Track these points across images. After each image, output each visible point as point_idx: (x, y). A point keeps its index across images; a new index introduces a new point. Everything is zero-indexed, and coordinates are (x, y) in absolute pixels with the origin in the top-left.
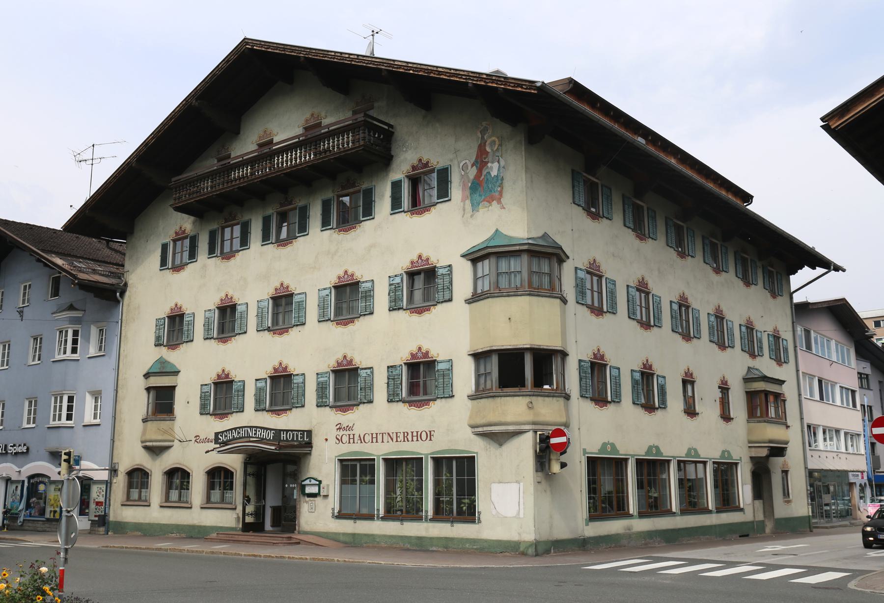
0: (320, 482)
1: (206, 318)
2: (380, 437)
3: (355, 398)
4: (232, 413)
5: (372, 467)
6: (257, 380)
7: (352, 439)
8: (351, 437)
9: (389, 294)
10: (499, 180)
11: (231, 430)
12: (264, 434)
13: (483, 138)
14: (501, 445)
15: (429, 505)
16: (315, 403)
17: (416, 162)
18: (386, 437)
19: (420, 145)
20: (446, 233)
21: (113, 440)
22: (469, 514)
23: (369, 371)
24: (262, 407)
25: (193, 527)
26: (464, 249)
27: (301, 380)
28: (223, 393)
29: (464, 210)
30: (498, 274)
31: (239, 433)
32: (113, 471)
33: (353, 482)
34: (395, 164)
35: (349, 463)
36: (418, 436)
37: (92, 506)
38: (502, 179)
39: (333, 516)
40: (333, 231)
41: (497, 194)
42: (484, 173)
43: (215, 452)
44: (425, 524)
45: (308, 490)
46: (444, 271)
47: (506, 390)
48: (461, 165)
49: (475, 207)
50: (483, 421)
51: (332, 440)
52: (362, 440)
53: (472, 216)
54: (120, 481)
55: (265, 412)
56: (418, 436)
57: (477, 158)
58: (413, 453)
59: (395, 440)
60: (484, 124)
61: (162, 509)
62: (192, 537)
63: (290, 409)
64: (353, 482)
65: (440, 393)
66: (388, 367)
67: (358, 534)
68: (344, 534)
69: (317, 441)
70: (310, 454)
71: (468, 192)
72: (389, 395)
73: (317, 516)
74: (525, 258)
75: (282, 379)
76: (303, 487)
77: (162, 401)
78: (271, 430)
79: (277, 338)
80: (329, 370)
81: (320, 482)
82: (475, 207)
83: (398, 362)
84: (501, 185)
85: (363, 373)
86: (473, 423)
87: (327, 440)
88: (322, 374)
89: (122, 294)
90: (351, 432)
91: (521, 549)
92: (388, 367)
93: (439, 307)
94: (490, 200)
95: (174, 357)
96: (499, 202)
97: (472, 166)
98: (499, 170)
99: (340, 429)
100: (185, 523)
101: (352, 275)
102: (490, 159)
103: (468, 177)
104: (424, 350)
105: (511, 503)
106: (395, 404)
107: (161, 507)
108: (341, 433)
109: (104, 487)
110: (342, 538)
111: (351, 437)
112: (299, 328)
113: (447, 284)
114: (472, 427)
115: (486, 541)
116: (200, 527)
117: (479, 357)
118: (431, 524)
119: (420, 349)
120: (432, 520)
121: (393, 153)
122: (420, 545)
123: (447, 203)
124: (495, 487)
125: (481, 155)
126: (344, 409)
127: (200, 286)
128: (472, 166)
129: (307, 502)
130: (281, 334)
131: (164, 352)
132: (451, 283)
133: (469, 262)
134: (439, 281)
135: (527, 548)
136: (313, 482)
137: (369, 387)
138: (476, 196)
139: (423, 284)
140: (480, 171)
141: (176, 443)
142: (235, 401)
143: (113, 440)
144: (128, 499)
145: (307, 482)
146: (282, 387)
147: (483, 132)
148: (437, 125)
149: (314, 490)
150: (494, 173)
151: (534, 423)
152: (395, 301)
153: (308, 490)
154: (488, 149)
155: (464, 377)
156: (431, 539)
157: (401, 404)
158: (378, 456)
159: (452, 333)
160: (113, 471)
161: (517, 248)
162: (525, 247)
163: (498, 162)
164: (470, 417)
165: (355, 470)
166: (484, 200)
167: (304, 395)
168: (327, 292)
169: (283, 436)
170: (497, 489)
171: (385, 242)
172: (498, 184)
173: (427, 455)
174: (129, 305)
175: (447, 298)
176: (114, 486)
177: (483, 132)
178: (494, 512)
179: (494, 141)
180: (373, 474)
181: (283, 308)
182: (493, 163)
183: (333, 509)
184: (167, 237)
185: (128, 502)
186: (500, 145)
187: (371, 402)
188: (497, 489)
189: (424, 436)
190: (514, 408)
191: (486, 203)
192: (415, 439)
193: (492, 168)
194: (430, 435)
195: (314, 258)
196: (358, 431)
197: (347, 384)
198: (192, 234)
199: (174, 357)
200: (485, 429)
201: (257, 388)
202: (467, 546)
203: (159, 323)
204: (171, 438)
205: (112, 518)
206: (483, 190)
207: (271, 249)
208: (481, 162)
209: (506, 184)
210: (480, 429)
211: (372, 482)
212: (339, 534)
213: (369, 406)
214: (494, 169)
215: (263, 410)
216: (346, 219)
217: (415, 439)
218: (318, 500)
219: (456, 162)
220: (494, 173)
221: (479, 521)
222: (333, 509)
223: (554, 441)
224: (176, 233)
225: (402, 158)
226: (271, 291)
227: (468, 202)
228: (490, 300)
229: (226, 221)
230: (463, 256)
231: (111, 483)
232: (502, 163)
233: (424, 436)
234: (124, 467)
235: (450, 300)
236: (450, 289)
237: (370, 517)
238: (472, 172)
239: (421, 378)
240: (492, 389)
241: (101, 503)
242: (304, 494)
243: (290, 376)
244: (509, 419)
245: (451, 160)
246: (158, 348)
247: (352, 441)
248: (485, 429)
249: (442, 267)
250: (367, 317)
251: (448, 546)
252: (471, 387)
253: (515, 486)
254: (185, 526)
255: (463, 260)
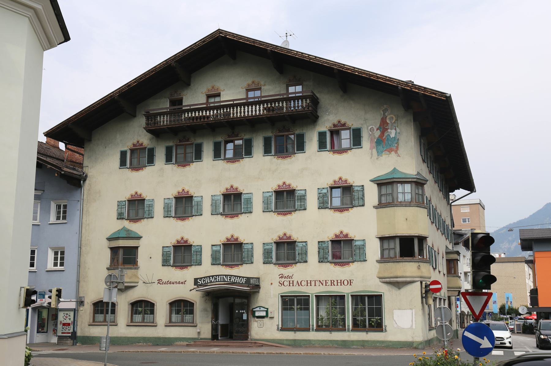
0: (267, 309)
1: (165, 203)
2: (313, 283)
3: (295, 259)
4: (191, 265)
5: (308, 300)
6: (213, 245)
7: (291, 284)
8: (291, 282)
9: (318, 199)
10: (396, 140)
11: (209, 277)
12: (238, 280)
13: (384, 114)
14: (399, 288)
15: (349, 322)
16: (261, 261)
17: (336, 122)
18: (317, 283)
19: (335, 112)
20: (361, 166)
21: (78, 281)
22: (378, 326)
23: (304, 244)
24: (218, 262)
25: (159, 339)
26: (373, 177)
27: (251, 247)
28: (182, 254)
29: (372, 154)
30: (392, 194)
31: (215, 279)
32: (81, 303)
33: (292, 309)
34: (320, 121)
35: (303, 298)
36: (342, 283)
37: (60, 327)
38: (398, 140)
39: (278, 329)
40: (272, 157)
41: (395, 148)
42: (386, 134)
43: (195, 290)
44: (348, 333)
45: (257, 314)
46: (359, 189)
47: (405, 258)
48: (369, 128)
49: (379, 153)
51: (276, 284)
52: (300, 284)
53: (377, 159)
54: (87, 311)
55: (220, 266)
56: (342, 283)
57: (380, 125)
58: (334, 292)
59: (324, 284)
60: (385, 106)
61: (129, 327)
62: (158, 345)
63: (242, 264)
64: (292, 309)
65: (358, 258)
66: (319, 242)
67: (298, 340)
68: (287, 340)
69: (264, 285)
70: (258, 292)
71: (374, 145)
72: (320, 258)
74: (414, 185)
75: (286, 245)
76: (253, 313)
77: (124, 255)
78: (243, 277)
79: (229, 220)
80: (273, 242)
81: (267, 309)
82: (379, 153)
83: (326, 239)
84: (397, 143)
86: (381, 276)
87: (272, 284)
88: (267, 244)
89: (85, 180)
90: (291, 280)
91: (414, 346)
92: (319, 242)
93: (355, 209)
94: (390, 151)
95: (135, 227)
96: (396, 152)
97: (377, 129)
98: (396, 134)
99: (282, 277)
100: (151, 336)
101: (289, 185)
102: (390, 127)
103: (374, 136)
104: (185, 239)
105: (405, 320)
106: (324, 263)
107: (128, 326)
108: (283, 280)
109: (72, 314)
110: (285, 342)
111: (291, 282)
112: (247, 215)
113: (361, 196)
114: (380, 278)
115: (390, 342)
116: (166, 338)
117: (382, 239)
118: (352, 333)
119: (182, 238)
120: (352, 330)
121: (318, 114)
123: (360, 149)
124: (397, 313)
125: (383, 124)
126: (285, 265)
127: (160, 181)
128: (377, 129)
129: (256, 321)
130: (232, 217)
131: (126, 224)
132: (363, 195)
133: (376, 185)
134: (355, 194)
135: (419, 345)
136: (262, 309)
137: (305, 253)
138: (380, 147)
139: (347, 194)
140: (383, 133)
141: (140, 284)
142: (194, 258)
143: (78, 281)
144: (94, 321)
145: (258, 309)
146: (234, 251)
147: (385, 111)
148: (351, 102)
149: (264, 314)
150: (393, 135)
151: (421, 277)
152: (323, 203)
153: (257, 314)
154: (388, 121)
155: (373, 250)
156: (352, 341)
157: (328, 264)
158: (312, 294)
159: (365, 224)
160: (81, 303)
161: (410, 180)
162: (415, 180)
163: (395, 129)
164: (379, 272)
165: (288, 302)
166: (386, 150)
167: (252, 256)
168: (270, 194)
169: (252, 281)
170: (397, 313)
171: (312, 168)
172: (395, 142)
173: (348, 294)
174: (89, 190)
175: (361, 204)
176: (80, 313)
177: (385, 111)
178: (395, 326)
179: (392, 118)
180: (308, 304)
181: (233, 202)
182: (391, 129)
183: (278, 326)
184: (127, 146)
185: (94, 323)
186: (397, 120)
187: (306, 262)
188: (397, 313)
189: (346, 283)
190: (408, 269)
191: (387, 152)
193: (391, 133)
194: (350, 282)
195: (259, 172)
196: (295, 279)
197: (286, 251)
198: (150, 146)
199: (135, 227)
200: (392, 279)
201: (213, 251)
202: (378, 345)
203: (120, 204)
204: (136, 281)
205: (79, 334)
206: (384, 144)
207: (220, 164)
208: (383, 127)
209: (401, 143)
210: (383, 280)
211: (308, 309)
212: (284, 340)
213: (305, 264)
214: (392, 133)
215: (219, 264)
216: (283, 151)
218: (265, 320)
219: (365, 126)
220: (393, 135)
221: (386, 331)
222: (278, 326)
223: (432, 287)
224: (134, 145)
225: (326, 118)
226: (223, 190)
227: (374, 151)
228: (395, 208)
229: (180, 141)
230: (371, 181)
231: (78, 311)
232: (398, 130)
233: (346, 283)
234: (90, 298)
235: (363, 205)
236: (363, 198)
237: (308, 330)
238: (378, 133)
239: (341, 249)
240: (395, 257)
241: (69, 324)
242: (254, 316)
243: (241, 244)
244: (408, 274)
245: (362, 124)
246: (120, 221)
248: (392, 279)
249: (357, 186)
250: (301, 211)
251: (363, 345)
252: (378, 256)
253: (409, 311)
254: (151, 338)
255: (372, 184)
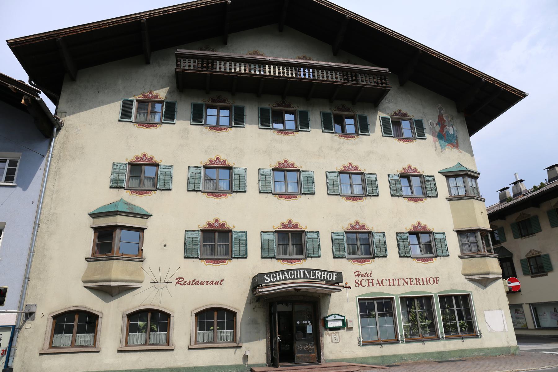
7: (370, 283)
8: (370, 281)
13: (440, 112)
14: (485, 286)
15: (440, 328)
29: (436, 147)
36: (428, 281)
42: (445, 130)
45: (330, 325)
46: (430, 179)
48: (429, 122)
50: (482, 271)
52: (381, 283)
56: (428, 281)
57: (439, 121)
59: (409, 283)
67: (387, 356)
73: (339, 346)
76: (325, 322)
84: (456, 140)
85: (377, 236)
91: (512, 352)
97: (437, 124)
99: (358, 275)
103: (435, 130)
108: (360, 278)
111: (370, 281)
113: (433, 186)
114: (465, 275)
115: (488, 349)
117: (461, 233)
122: (442, 359)
126: (361, 260)
128: (437, 124)
129: (329, 335)
145: (332, 318)
150: (451, 132)
153: (330, 325)
158: (397, 296)
164: (464, 269)
167: (319, 248)
177: (440, 109)
183: (359, 339)
187: (386, 256)
192: (425, 283)
193: (449, 129)
194: (436, 280)
196: (375, 277)
210: (470, 277)
212: (368, 358)
213: (384, 259)
217: (425, 283)
218: (342, 332)
227: (438, 143)
238: (438, 128)
247: (371, 284)
250: (372, 198)
253: (499, 311)
